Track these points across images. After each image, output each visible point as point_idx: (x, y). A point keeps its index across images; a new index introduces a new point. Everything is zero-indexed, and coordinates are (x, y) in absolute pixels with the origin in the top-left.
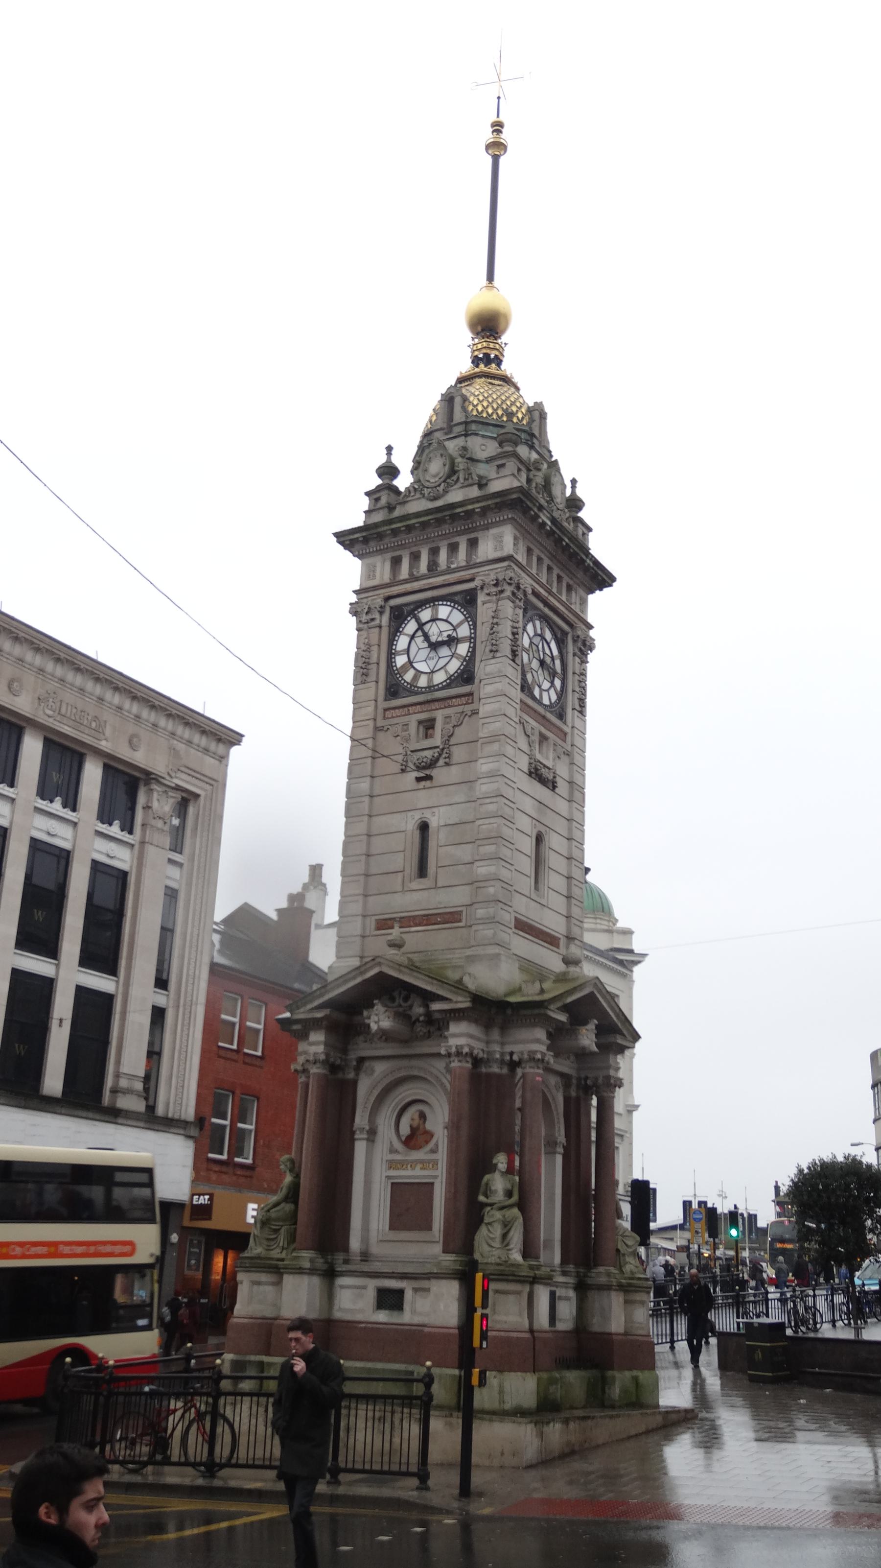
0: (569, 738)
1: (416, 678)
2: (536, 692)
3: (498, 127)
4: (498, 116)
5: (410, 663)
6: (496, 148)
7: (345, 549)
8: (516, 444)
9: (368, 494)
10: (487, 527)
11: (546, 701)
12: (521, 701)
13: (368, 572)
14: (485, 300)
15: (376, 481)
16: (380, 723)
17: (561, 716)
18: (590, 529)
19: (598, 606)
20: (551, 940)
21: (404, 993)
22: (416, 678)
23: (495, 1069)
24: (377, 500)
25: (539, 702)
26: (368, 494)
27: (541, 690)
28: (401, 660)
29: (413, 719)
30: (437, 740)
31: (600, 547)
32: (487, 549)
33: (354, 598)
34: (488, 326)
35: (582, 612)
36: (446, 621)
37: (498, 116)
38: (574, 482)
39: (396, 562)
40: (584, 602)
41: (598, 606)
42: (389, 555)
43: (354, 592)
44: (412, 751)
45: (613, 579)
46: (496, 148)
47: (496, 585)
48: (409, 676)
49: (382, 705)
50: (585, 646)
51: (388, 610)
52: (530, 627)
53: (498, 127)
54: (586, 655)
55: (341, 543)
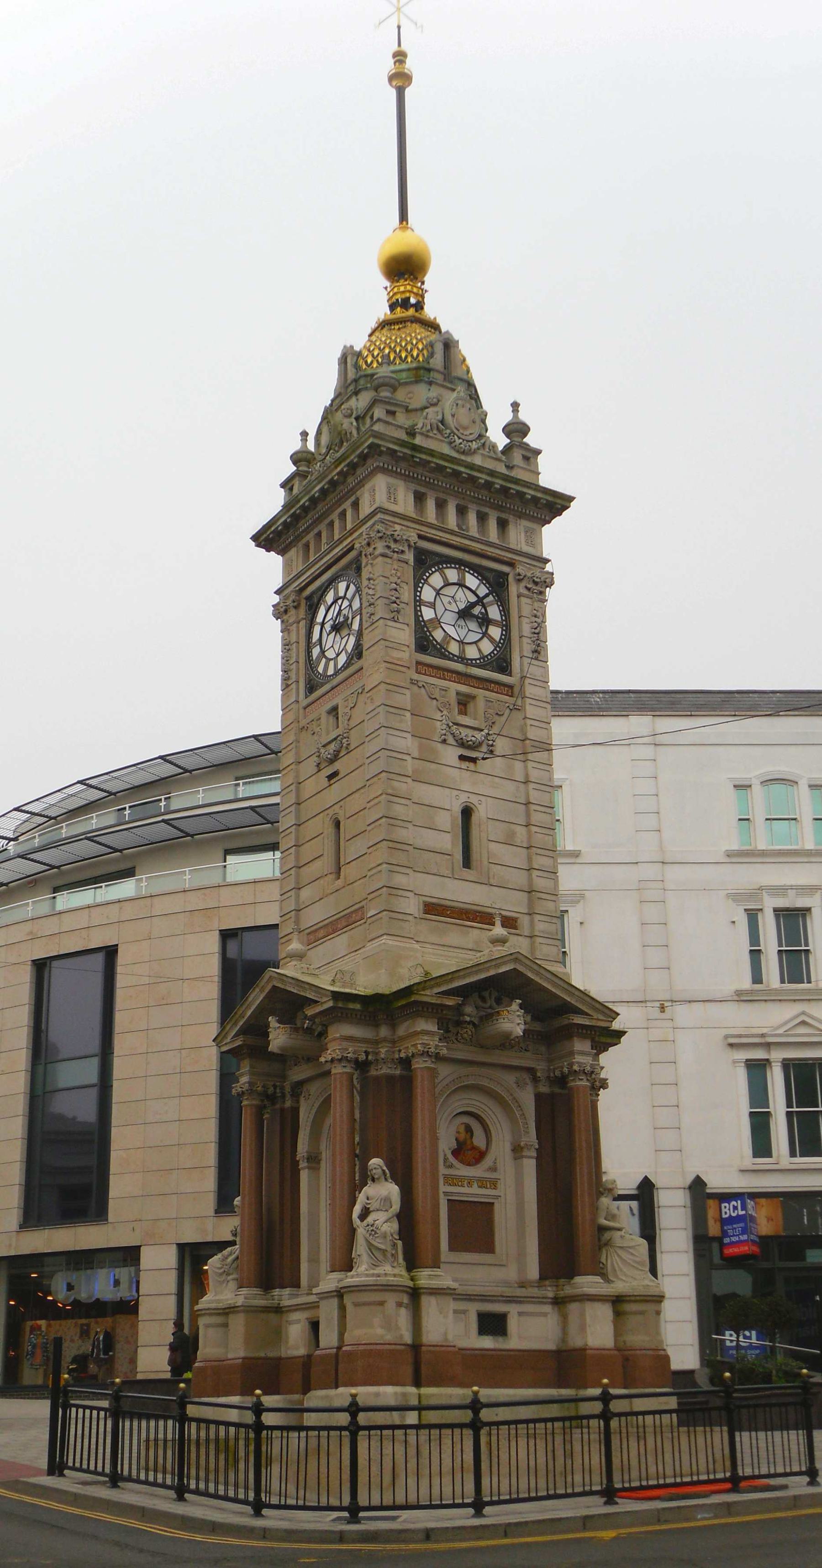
0: (516, 690)
1: (326, 668)
2: (454, 648)
3: (400, 57)
4: (399, 45)
5: (323, 652)
6: (400, 80)
7: (268, 550)
8: (394, 389)
10: (361, 484)
13: (287, 566)
14: (402, 242)
16: (303, 723)
22: (326, 668)
23: (385, 1070)
24: (291, 489)
25: (462, 659)
28: (316, 651)
32: (366, 509)
33: (276, 599)
34: (405, 268)
35: (533, 546)
37: (399, 45)
40: (534, 538)
42: (300, 544)
43: (275, 593)
44: (324, 746)
45: (571, 499)
46: (400, 80)
47: (369, 544)
49: (304, 702)
50: (541, 584)
51: (303, 602)
53: (400, 57)
54: (542, 593)
55: (258, 545)
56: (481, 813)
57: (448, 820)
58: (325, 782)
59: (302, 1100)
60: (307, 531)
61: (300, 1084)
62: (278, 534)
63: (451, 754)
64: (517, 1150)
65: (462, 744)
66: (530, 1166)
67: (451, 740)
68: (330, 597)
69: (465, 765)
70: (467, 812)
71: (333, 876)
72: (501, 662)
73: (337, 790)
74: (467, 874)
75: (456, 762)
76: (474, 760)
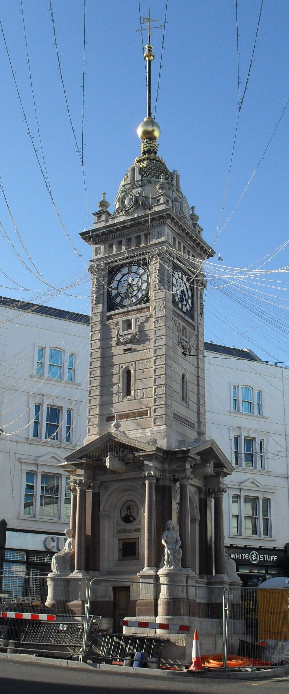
9: (95, 214)
11: (185, 310)
12: (173, 310)
13: (97, 252)
15: (98, 209)
17: (192, 318)
18: (202, 230)
19: (207, 266)
20: (191, 425)
21: (122, 449)
26: (95, 214)
27: (182, 305)
29: (120, 320)
30: (134, 330)
31: (207, 237)
36: (135, 273)
38: (193, 208)
39: (111, 246)
41: (207, 266)
48: (118, 300)
52: (176, 276)
56: (188, 378)
57: (179, 379)
58: (123, 352)
59: (102, 490)
60: (113, 239)
61: (103, 482)
62: (97, 236)
63: (181, 350)
64: (193, 520)
65: (183, 348)
66: (197, 526)
67: (180, 346)
68: (125, 270)
69: (184, 356)
70: (183, 376)
71: (125, 394)
72: (191, 313)
73: (130, 357)
74: (182, 402)
75: (181, 354)
76: (185, 355)
